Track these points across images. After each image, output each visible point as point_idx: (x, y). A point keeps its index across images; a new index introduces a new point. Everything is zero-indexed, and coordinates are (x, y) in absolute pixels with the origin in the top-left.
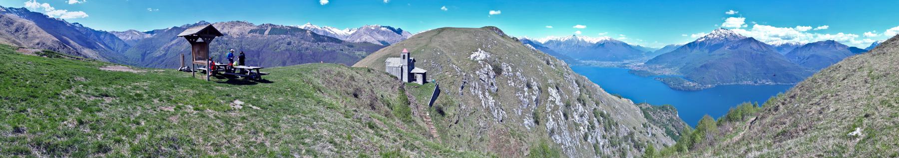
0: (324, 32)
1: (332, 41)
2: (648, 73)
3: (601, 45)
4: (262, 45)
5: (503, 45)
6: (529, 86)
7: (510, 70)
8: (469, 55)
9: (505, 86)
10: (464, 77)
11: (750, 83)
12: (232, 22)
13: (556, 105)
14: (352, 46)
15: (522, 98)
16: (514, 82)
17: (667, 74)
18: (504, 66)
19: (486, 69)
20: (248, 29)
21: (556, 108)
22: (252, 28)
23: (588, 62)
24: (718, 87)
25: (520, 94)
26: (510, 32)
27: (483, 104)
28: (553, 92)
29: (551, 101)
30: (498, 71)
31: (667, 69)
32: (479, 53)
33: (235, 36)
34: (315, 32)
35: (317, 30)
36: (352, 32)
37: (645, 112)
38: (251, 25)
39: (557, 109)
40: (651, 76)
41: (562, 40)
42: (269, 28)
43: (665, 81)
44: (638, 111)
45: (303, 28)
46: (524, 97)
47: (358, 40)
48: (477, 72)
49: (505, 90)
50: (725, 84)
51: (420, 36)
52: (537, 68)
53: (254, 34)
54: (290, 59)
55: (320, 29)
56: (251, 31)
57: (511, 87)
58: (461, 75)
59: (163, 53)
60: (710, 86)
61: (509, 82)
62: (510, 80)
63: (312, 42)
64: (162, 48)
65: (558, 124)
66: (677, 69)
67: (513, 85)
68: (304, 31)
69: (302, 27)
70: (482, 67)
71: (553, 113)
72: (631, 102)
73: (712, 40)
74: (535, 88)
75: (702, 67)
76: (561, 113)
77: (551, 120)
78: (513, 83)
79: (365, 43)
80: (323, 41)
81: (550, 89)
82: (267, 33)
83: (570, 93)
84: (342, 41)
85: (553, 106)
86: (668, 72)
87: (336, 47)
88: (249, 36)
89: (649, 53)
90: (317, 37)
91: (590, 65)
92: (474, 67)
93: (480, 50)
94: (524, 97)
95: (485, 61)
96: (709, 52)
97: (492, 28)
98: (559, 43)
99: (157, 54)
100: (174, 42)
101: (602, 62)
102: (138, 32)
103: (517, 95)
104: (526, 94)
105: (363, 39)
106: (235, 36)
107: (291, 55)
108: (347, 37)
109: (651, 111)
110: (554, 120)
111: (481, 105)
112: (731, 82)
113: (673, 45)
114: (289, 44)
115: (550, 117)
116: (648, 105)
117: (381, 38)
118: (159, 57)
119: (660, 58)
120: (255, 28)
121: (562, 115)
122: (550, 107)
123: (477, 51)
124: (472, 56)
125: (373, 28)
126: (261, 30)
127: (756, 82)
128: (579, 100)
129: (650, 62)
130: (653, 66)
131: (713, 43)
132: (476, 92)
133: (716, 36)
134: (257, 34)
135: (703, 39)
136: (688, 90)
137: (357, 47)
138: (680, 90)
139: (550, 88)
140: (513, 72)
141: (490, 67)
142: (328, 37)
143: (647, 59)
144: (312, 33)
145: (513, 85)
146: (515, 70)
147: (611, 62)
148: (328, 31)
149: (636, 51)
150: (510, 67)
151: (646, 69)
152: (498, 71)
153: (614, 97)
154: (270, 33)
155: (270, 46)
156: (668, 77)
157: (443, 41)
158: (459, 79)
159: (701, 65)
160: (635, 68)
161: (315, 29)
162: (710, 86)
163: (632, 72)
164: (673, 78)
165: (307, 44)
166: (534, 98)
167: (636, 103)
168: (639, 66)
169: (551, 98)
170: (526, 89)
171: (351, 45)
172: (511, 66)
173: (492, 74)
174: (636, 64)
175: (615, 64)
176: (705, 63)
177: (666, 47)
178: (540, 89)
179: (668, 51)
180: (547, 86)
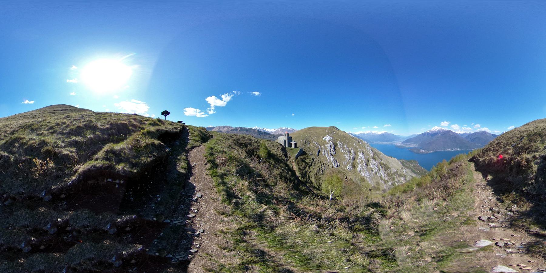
0: (263, 130)
1: (266, 134)
2: (403, 147)
5: (338, 134)
6: (350, 152)
8: (323, 138)
11: (450, 150)
12: (224, 126)
13: (362, 160)
14: (275, 136)
15: (346, 157)
16: (343, 150)
17: (413, 146)
18: (338, 142)
19: (330, 144)
21: (362, 161)
22: (232, 129)
23: (377, 142)
24: (436, 152)
26: (342, 129)
27: (328, 159)
28: (360, 154)
29: (360, 159)
31: (413, 145)
32: (327, 137)
34: (259, 130)
35: (260, 130)
36: (275, 130)
37: (402, 163)
38: (232, 127)
39: (362, 162)
40: (404, 148)
41: (365, 133)
42: (240, 129)
43: (411, 150)
44: (399, 163)
47: (278, 134)
48: (326, 146)
50: (439, 151)
51: (301, 130)
53: (233, 131)
55: (261, 129)
56: (232, 130)
58: (318, 146)
60: (432, 152)
61: (341, 150)
62: (341, 149)
65: (363, 168)
66: (417, 144)
68: (254, 130)
69: (254, 128)
70: (328, 143)
71: (360, 164)
72: (396, 159)
73: (432, 132)
74: (352, 153)
75: (428, 143)
76: (364, 164)
77: (360, 167)
80: (262, 134)
81: (359, 153)
82: (238, 130)
83: (368, 155)
84: (270, 134)
86: (413, 146)
88: (231, 132)
89: (403, 138)
91: (378, 143)
92: (324, 143)
93: (327, 135)
95: (330, 141)
97: (333, 127)
98: (364, 134)
105: (280, 133)
108: (273, 132)
109: (405, 162)
110: (361, 166)
111: (327, 160)
115: (359, 165)
116: (404, 161)
119: (409, 140)
120: (233, 129)
121: (365, 165)
122: (359, 161)
123: (326, 136)
124: (324, 138)
125: (284, 129)
126: (236, 129)
127: (452, 150)
128: (373, 158)
129: (404, 142)
131: (433, 133)
132: (325, 154)
133: (434, 130)
134: (234, 131)
135: (429, 131)
136: (423, 154)
138: (419, 154)
140: (342, 145)
141: (332, 143)
142: (265, 132)
143: (402, 141)
144: (258, 131)
146: (343, 145)
148: (265, 130)
150: (341, 144)
151: (402, 145)
152: (335, 145)
153: (388, 157)
154: (240, 131)
157: (311, 132)
158: (317, 149)
159: (428, 142)
160: (398, 145)
161: (259, 129)
162: (432, 152)
163: (396, 146)
164: (415, 148)
166: (352, 157)
167: (398, 159)
169: (359, 157)
172: (341, 143)
173: (333, 146)
174: (398, 143)
175: (389, 143)
177: (413, 135)
179: (414, 137)
180: (358, 152)
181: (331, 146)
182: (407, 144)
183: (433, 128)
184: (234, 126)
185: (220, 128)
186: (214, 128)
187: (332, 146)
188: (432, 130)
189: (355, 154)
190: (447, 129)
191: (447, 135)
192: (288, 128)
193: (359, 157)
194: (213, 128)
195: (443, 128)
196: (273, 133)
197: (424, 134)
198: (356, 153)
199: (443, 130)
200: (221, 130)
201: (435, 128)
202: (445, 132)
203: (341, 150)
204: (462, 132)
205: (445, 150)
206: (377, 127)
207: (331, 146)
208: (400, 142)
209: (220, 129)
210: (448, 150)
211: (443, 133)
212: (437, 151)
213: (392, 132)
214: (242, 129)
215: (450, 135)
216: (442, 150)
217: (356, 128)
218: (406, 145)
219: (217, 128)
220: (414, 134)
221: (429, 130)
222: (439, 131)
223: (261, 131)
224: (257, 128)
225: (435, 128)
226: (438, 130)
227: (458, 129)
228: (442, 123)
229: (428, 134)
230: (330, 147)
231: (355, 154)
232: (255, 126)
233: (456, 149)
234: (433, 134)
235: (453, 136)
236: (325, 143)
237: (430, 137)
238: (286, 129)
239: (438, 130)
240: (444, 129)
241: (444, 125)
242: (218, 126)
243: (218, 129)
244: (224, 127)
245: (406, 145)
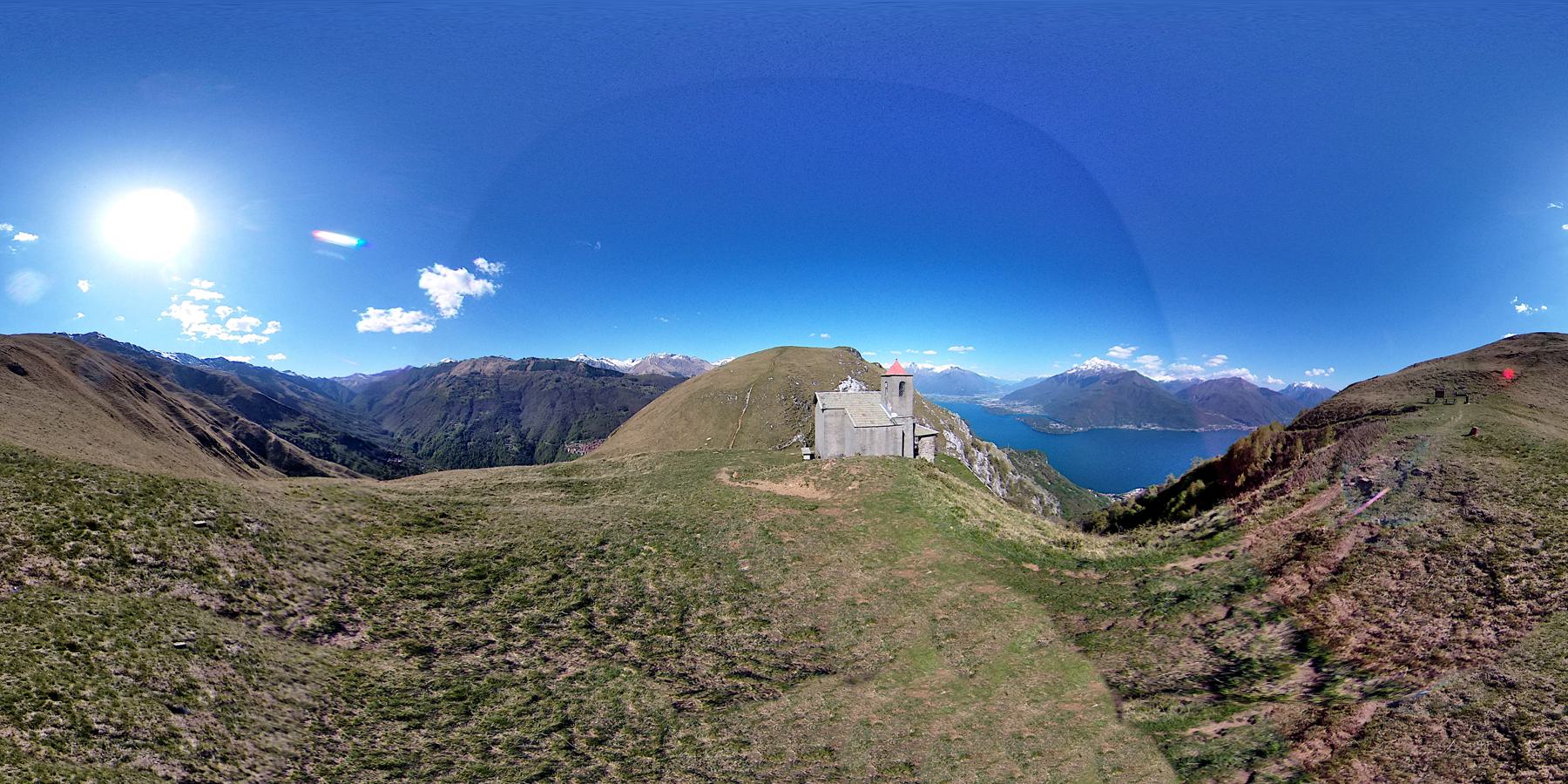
2: (1005, 411)
3: (946, 375)
4: (524, 384)
11: (1131, 427)
14: (636, 380)
20: (505, 365)
31: (1029, 407)
33: (489, 375)
35: (593, 362)
36: (635, 363)
38: (509, 360)
40: (1009, 415)
42: (532, 363)
43: (1026, 421)
45: (574, 360)
47: (644, 373)
54: (560, 401)
59: (395, 399)
63: (587, 377)
64: (393, 393)
68: (577, 363)
69: (574, 359)
73: (1085, 372)
75: (1072, 405)
79: (653, 375)
82: (529, 368)
86: (1029, 410)
87: (616, 381)
88: (507, 373)
89: (1005, 387)
90: (593, 371)
91: (932, 399)
96: (1082, 387)
99: (388, 400)
100: (413, 386)
102: (364, 375)
105: (650, 371)
106: (489, 375)
107: (561, 394)
112: (1109, 425)
113: (1035, 378)
114: (558, 380)
117: (673, 369)
118: (389, 406)
119: (1020, 394)
120: (514, 363)
125: (662, 357)
126: (522, 365)
127: (1139, 427)
129: (1007, 398)
130: (1012, 403)
133: (1090, 368)
134: (518, 371)
136: (1055, 434)
137: (643, 381)
138: (1044, 433)
144: (586, 366)
147: (958, 397)
149: (988, 385)
155: (535, 384)
156: (1030, 415)
159: (1070, 402)
160: (989, 405)
161: (589, 361)
163: (986, 410)
165: (580, 380)
168: (994, 402)
171: (635, 379)
174: (991, 401)
175: (964, 399)
176: (1077, 400)
182: (1017, 403)
183: (1087, 362)
184: (517, 357)
185: (474, 362)
186: (457, 363)
188: (1084, 367)
190: (1126, 367)
191: (1126, 386)
192: (672, 355)
194: (453, 365)
195: (1114, 365)
196: (631, 372)
197: (1059, 379)
199: (1115, 369)
200: (477, 369)
201: (1094, 364)
202: (1120, 375)
204: (1168, 379)
205: (1119, 427)
206: (935, 353)
208: (996, 398)
209: (473, 367)
210: (1126, 426)
211: (1115, 379)
212: (1096, 427)
213: (973, 367)
214: (539, 364)
215: (1134, 383)
216: (1110, 427)
217: (873, 354)
218: (1014, 406)
219: (467, 365)
220: (1033, 376)
221: (1075, 365)
222: (1103, 371)
223: (596, 366)
224: (581, 358)
225: (1094, 363)
226: (1100, 367)
227: (1155, 369)
228: (1116, 348)
229: (1072, 377)
232: (577, 352)
233: (1150, 425)
234: (1087, 380)
235: (1142, 387)
237: (1078, 386)
238: (668, 359)
239: (1100, 367)
240: (1117, 365)
241: (1118, 356)
242: (468, 358)
243: (469, 367)
244: (486, 360)
245: (1014, 406)
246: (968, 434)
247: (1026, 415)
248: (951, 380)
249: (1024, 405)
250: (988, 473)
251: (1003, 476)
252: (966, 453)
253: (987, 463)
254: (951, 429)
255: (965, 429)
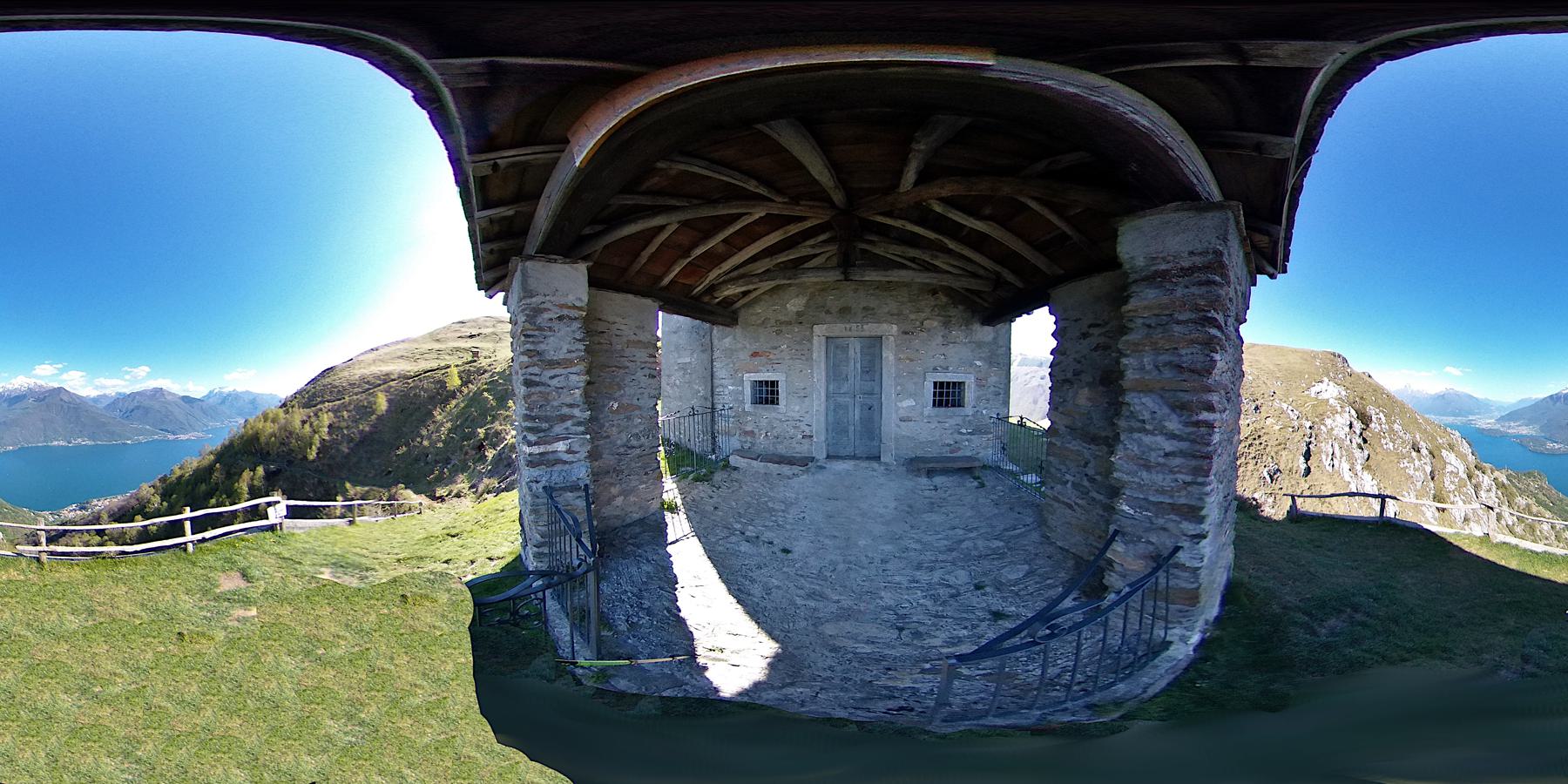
7: (1383, 419)
9: (1378, 450)
10: (1309, 431)
15: (1412, 472)
17: (1524, 432)
18: (1372, 410)
25: (1406, 464)
28: (1450, 457)
30: (1364, 418)
31: (1524, 428)
40: (1504, 436)
43: (1522, 441)
46: (1415, 470)
49: (1379, 457)
52: (1416, 419)
57: (1388, 452)
58: (1301, 426)
61: (1383, 441)
62: (1385, 438)
67: (1392, 448)
74: (1424, 451)
78: (1391, 444)
81: (1444, 453)
85: (1457, 480)
86: (1524, 431)
92: (1320, 410)
94: (1415, 470)
101: (1442, 418)
103: (1402, 466)
104: (1417, 462)
129: (1501, 419)
130: (1507, 424)
139: (1443, 451)
145: (1392, 448)
146: (1390, 422)
150: (1381, 415)
152: (1364, 418)
164: (1532, 438)
166: (1428, 469)
169: (1449, 468)
170: (1414, 454)
172: (1383, 412)
178: (1431, 453)
180: (1439, 447)
181: (1351, 426)
182: (1512, 424)
187: (1355, 423)
189: (1434, 457)
193: (1448, 466)
198: (1435, 453)
203: (1383, 441)
207: (1351, 426)
230: (1347, 429)
231: (1434, 457)
236: (1321, 411)
245: (1509, 427)
246: (1471, 455)
247: (1522, 436)
248: (1446, 403)
249: (1520, 426)
250: (1497, 500)
251: (1511, 502)
252: (1470, 477)
253: (1494, 489)
254: (1451, 447)
255: (1466, 449)
